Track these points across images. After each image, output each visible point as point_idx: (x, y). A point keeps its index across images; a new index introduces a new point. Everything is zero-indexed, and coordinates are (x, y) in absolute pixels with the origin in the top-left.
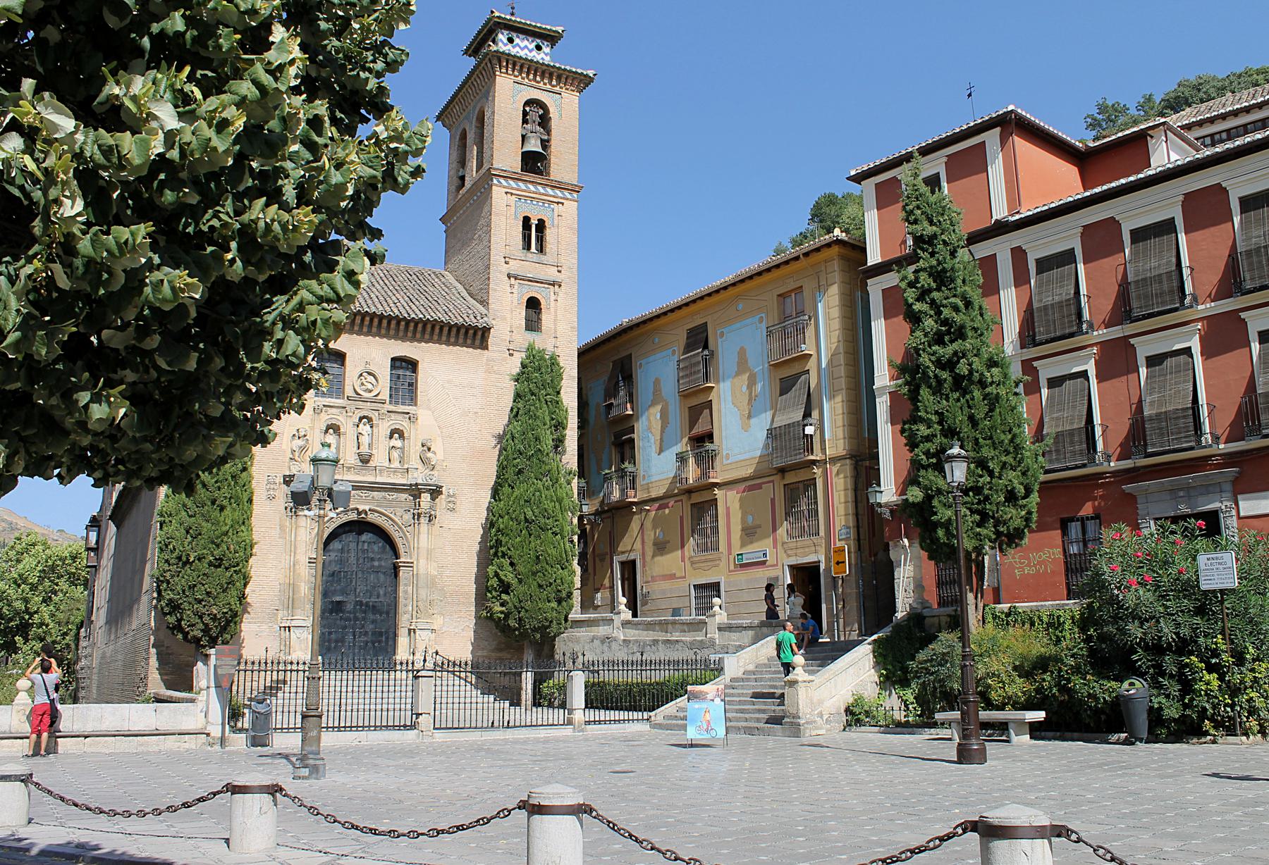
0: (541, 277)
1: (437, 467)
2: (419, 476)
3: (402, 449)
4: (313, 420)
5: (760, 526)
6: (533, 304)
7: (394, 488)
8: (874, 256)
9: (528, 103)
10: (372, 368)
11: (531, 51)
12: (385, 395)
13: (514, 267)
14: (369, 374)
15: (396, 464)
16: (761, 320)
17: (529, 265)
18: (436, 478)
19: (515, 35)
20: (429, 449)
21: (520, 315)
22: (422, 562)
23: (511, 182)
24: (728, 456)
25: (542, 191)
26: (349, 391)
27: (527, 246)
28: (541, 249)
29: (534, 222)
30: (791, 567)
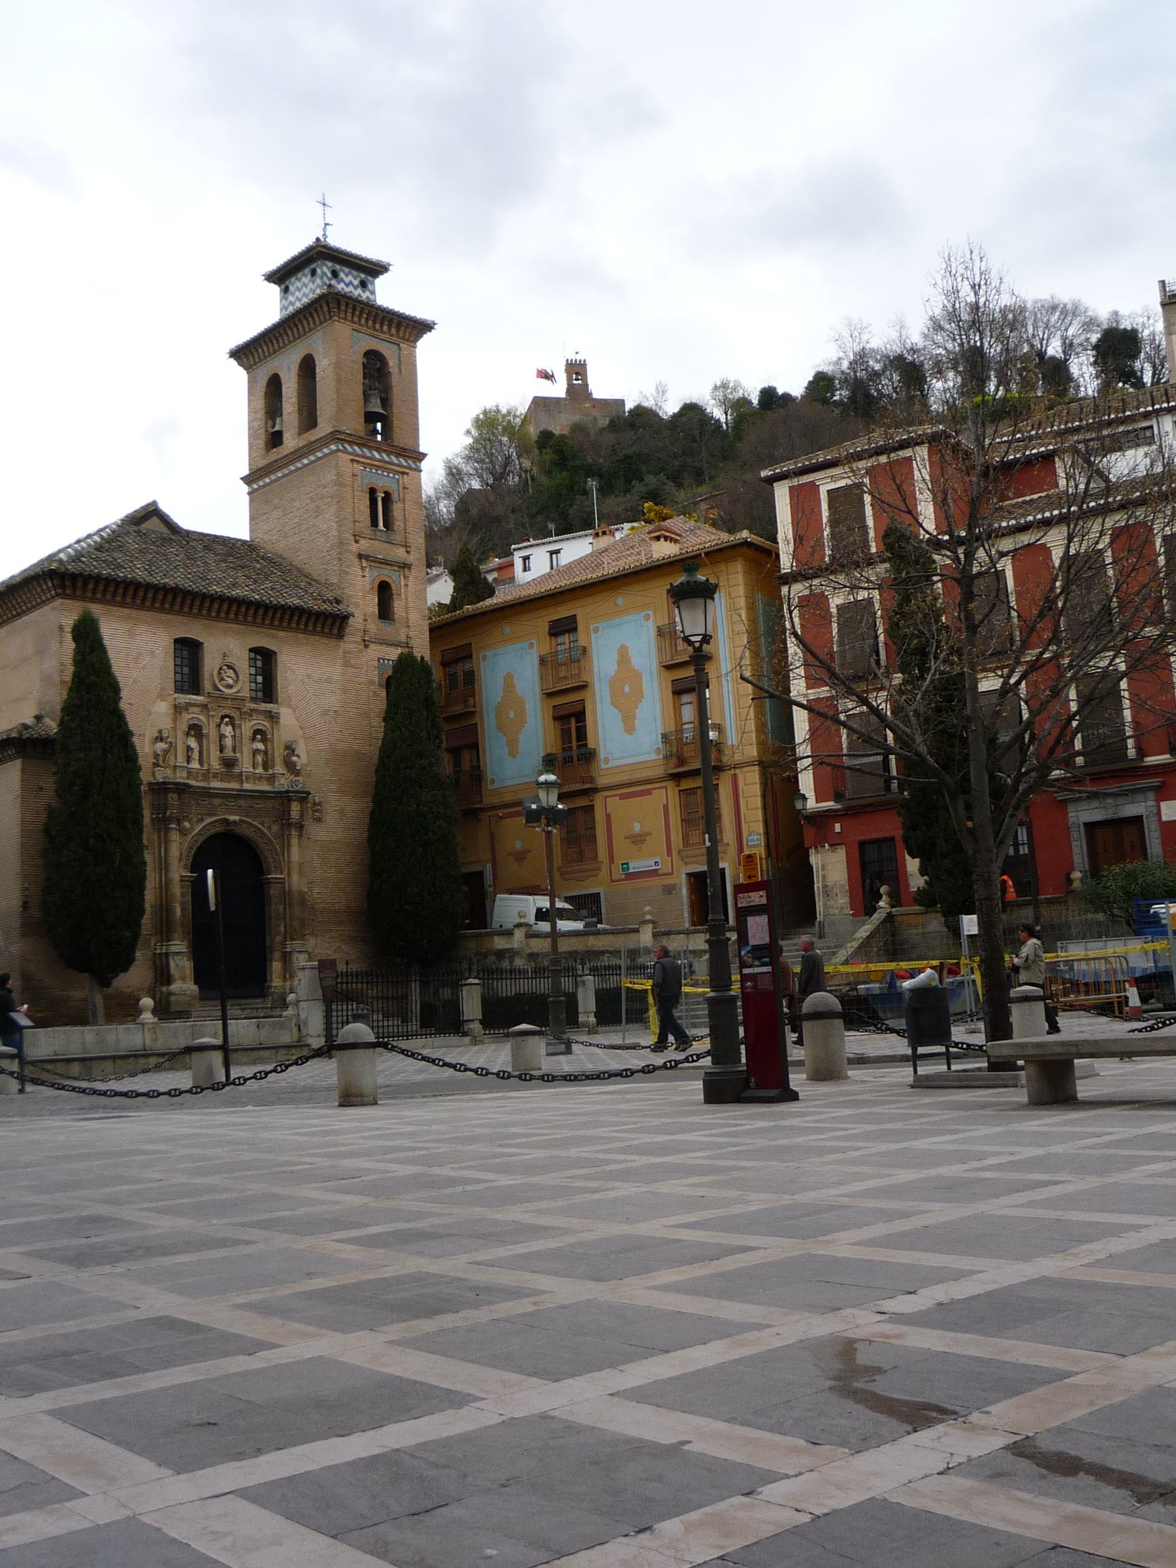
0: (391, 557)
1: (303, 773)
2: (284, 783)
3: (266, 753)
4: (175, 720)
5: (650, 834)
6: (384, 591)
7: (262, 795)
8: (786, 563)
10: (229, 660)
11: (356, 288)
12: (246, 693)
14: (229, 667)
15: (260, 770)
16: (647, 618)
18: (301, 782)
19: (338, 267)
20: (293, 751)
21: (371, 604)
22: (295, 877)
23: (356, 448)
24: (607, 760)
25: (386, 458)
26: (207, 686)
27: (374, 523)
30: (688, 875)
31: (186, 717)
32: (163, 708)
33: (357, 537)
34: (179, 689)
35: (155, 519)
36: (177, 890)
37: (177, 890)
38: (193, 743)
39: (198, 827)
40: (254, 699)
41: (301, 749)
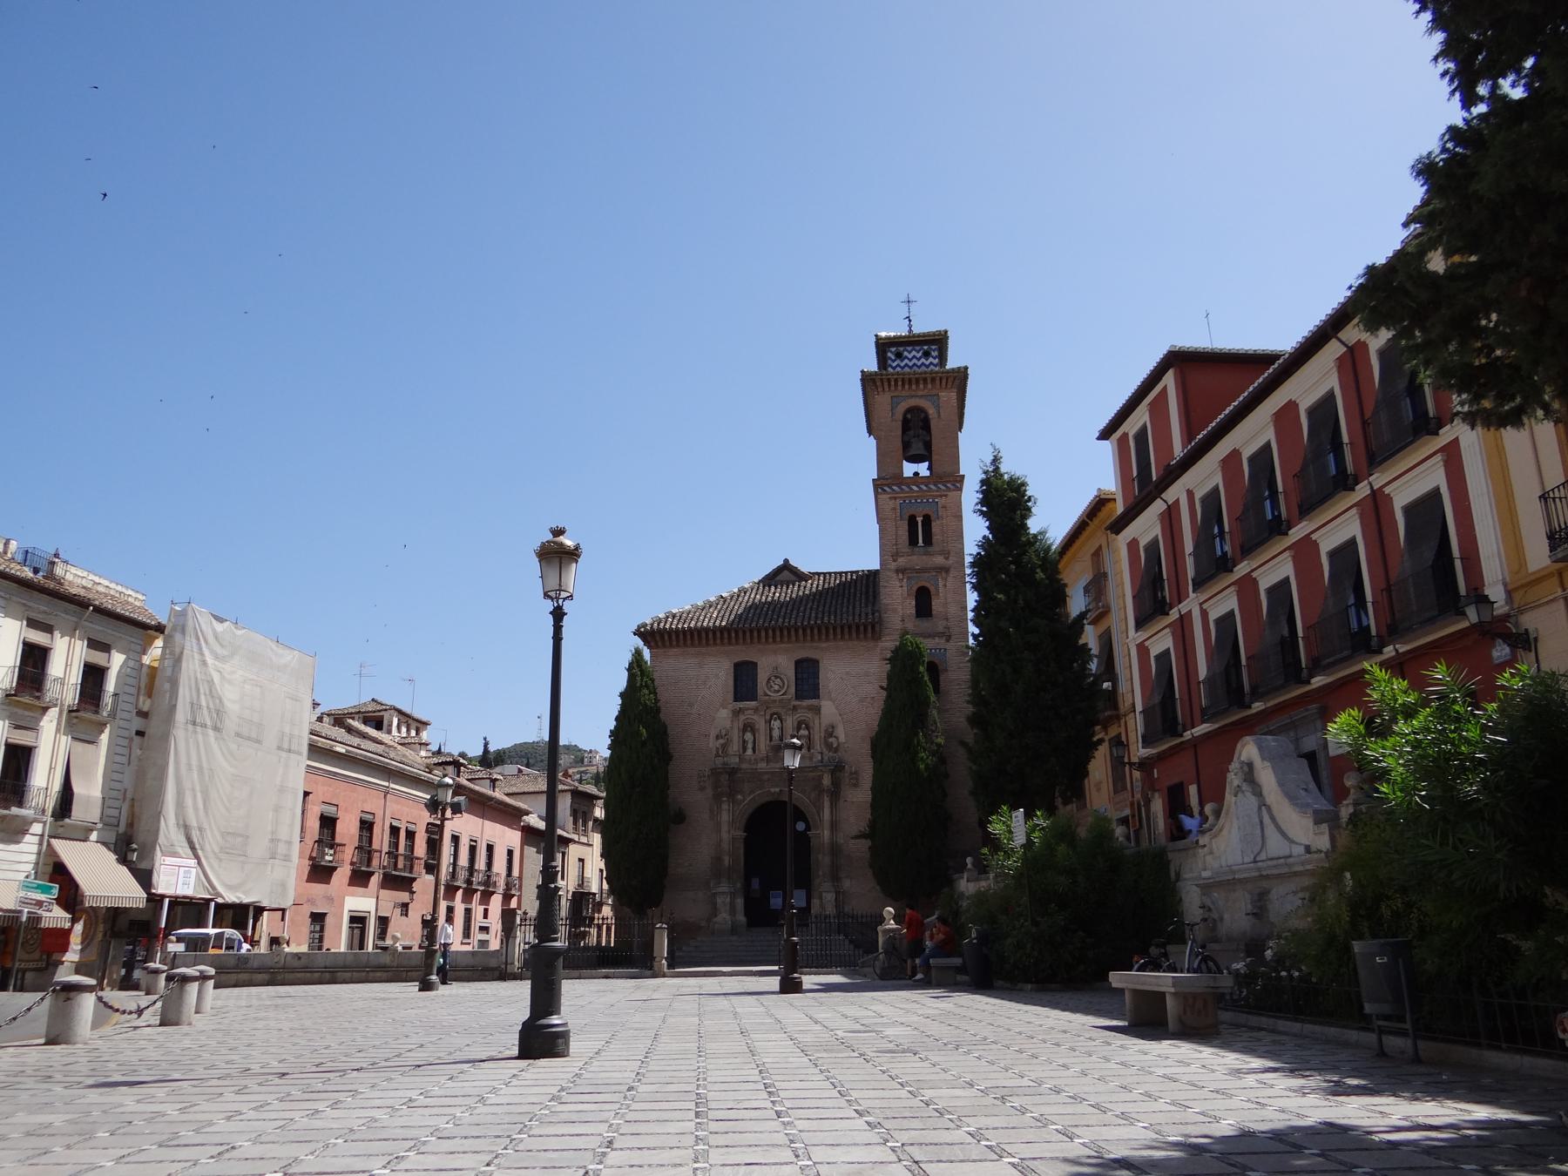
9: (909, 411)
13: (902, 561)
17: (917, 560)
21: (910, 606)
26: (760, 692)
27: (913, 541)
28: (928, 540)
29: (919, 520)
31: (742, 718)
32: (724, 715)
33: (895, 556)
34: (736, 700)
35: (786, 573)
36: (725, 846)
37: (725, 846)
38: (748, 736)
39: (749, 799)
40: (798, 697)
41: (840, 732)
